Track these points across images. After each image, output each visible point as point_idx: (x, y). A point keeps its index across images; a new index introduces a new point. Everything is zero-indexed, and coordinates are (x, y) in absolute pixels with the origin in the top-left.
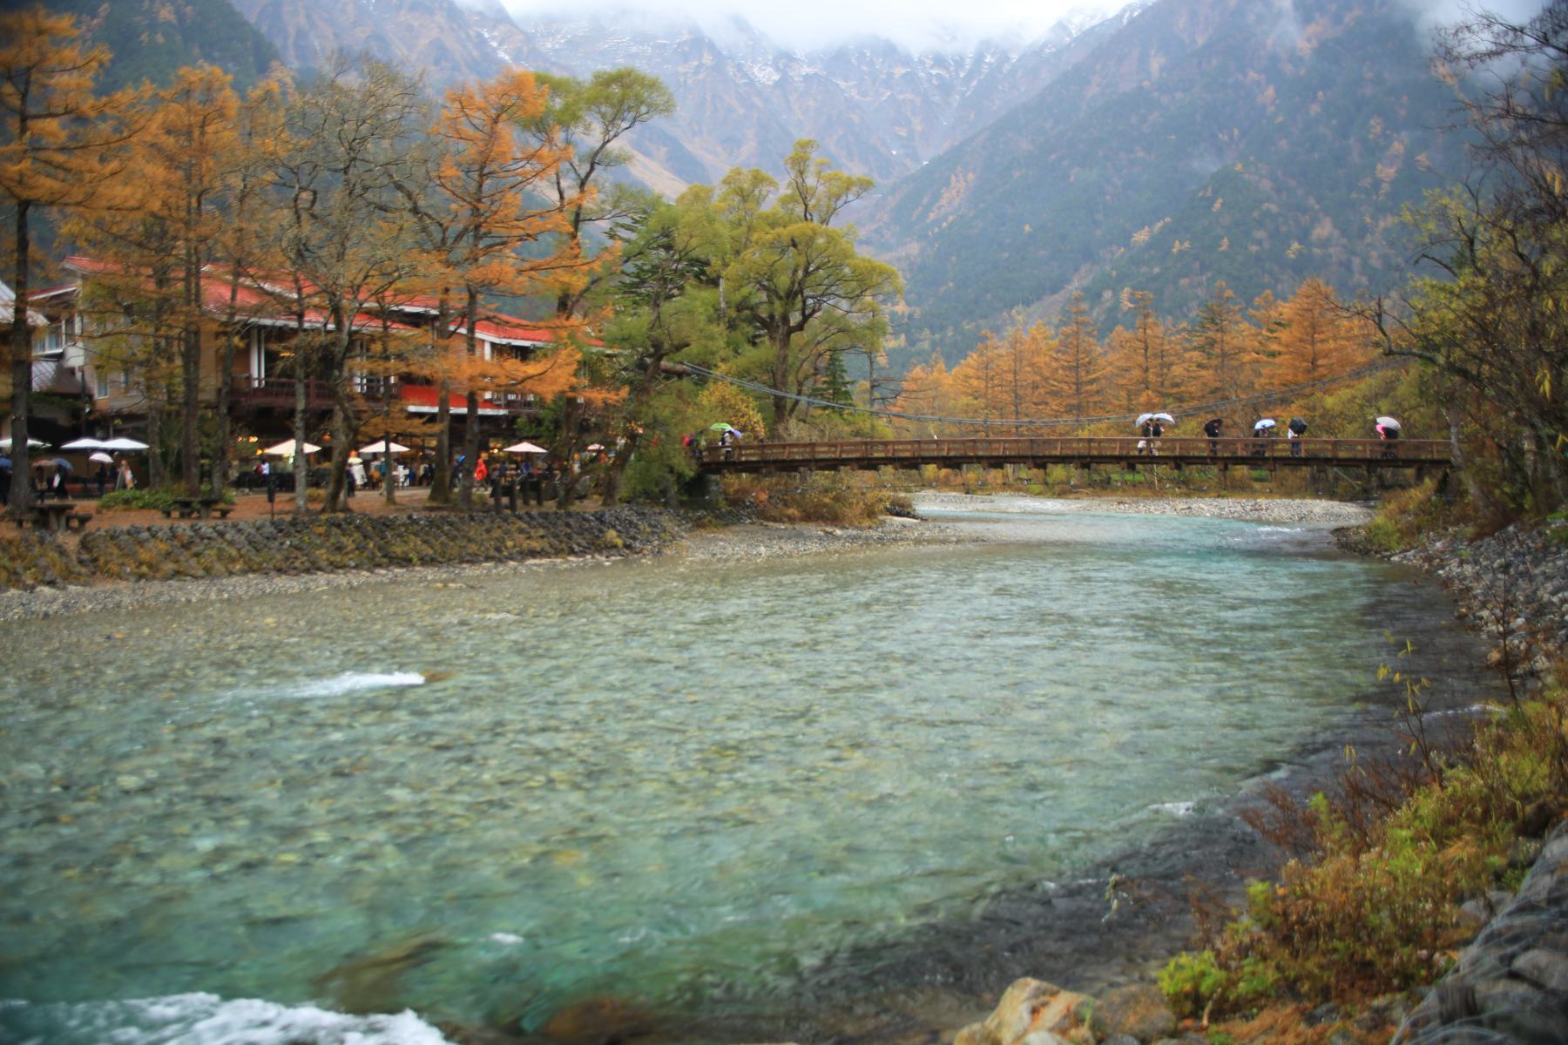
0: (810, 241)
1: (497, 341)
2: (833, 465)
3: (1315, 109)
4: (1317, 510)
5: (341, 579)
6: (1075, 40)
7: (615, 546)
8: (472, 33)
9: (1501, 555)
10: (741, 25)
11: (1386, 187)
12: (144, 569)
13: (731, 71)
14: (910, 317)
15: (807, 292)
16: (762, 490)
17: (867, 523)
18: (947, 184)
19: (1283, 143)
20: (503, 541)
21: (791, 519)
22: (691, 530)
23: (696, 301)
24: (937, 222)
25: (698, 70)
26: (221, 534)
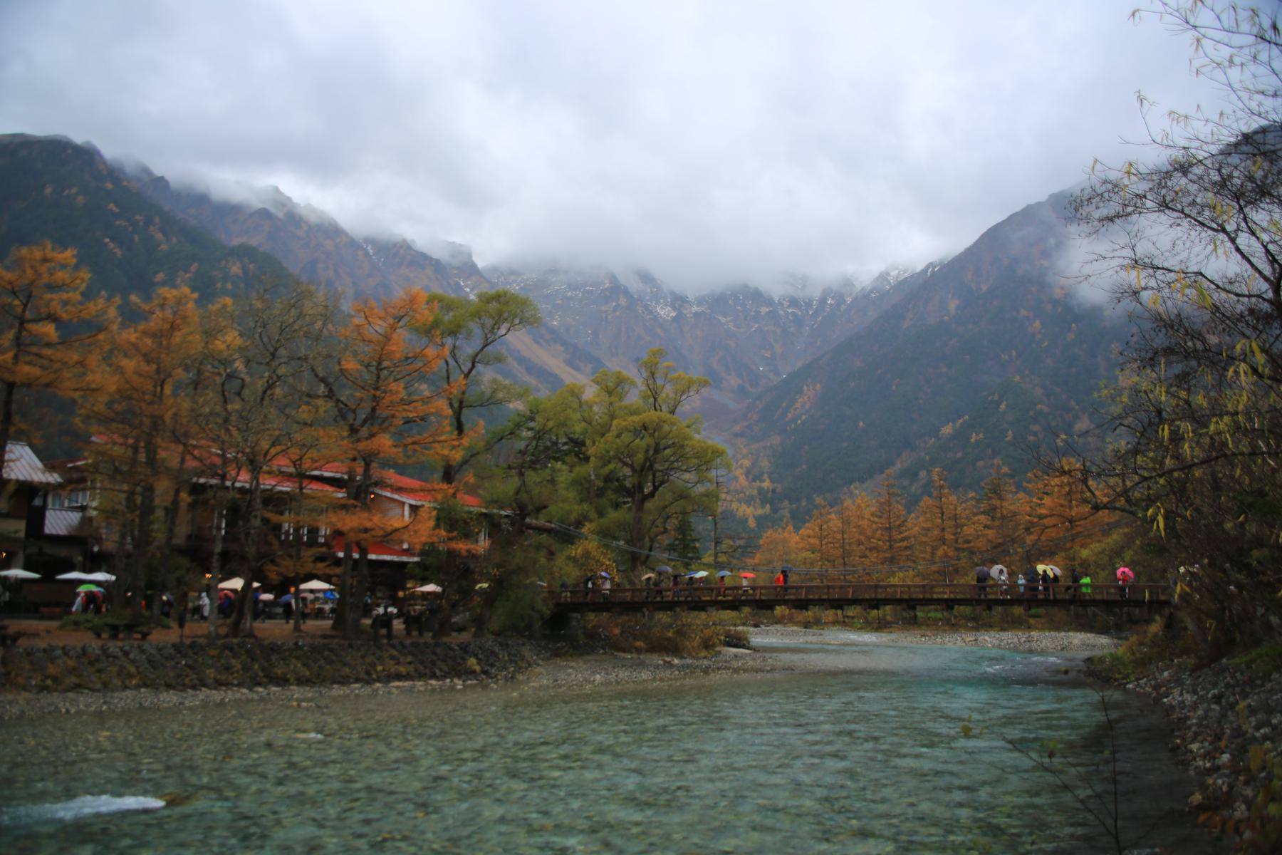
0: (658, 427)
1: (413, 502)
2: (669, 606)
3: (1070, 337)
4: (1076, 641)
5: (229, 695)
6: (892, 287)
7: (474, 672)
8: (452, 282)
9: (1215, 685)
10: (646, 278)
12: (49, 682)
13: (640, 310)
14: (774, 491)
15: (657, 466)
16: (617, 625)
17: (704, 653)
19: (1049, 361)
20: (374, 666)
21: (639, 650)
22: (548, 659)
23: (564, 473)
26: (126, 654)
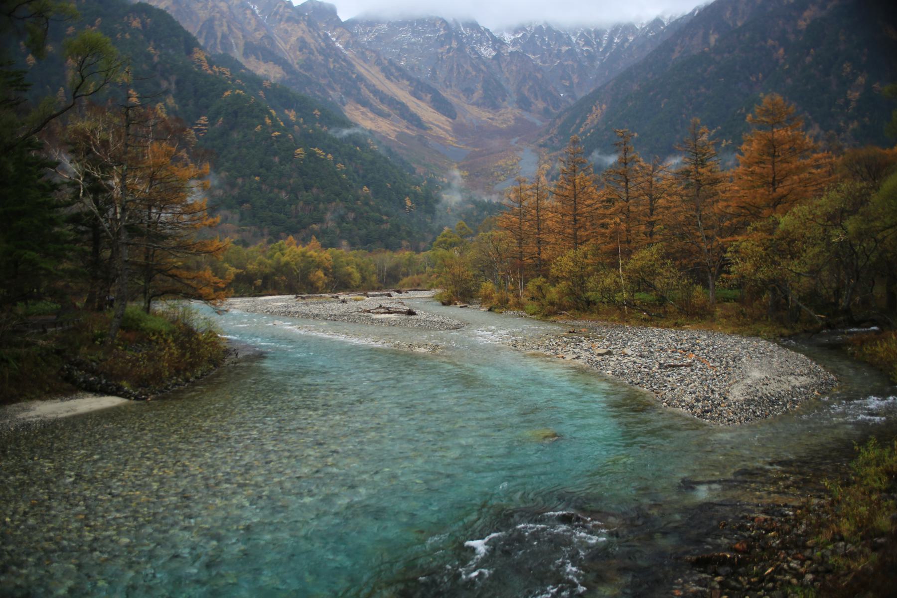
6: (667, 28)
13: (468, 50)
18: (591, 111)
19: (789, 81)
24: (584, 133)
25: (448, 51)
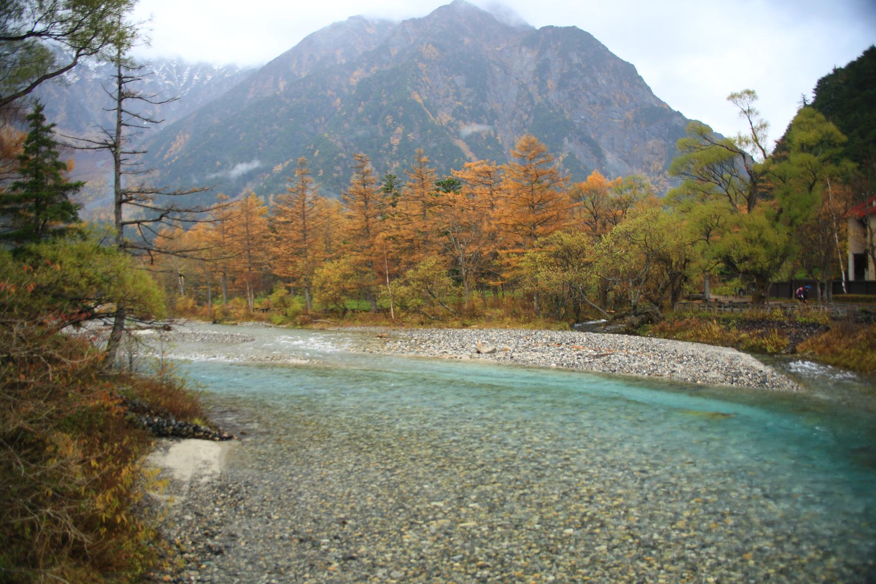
3: (360, 110)
11: (395, 148)
18: (174, 139)
19: (346, 125)
24: (169, 159)
